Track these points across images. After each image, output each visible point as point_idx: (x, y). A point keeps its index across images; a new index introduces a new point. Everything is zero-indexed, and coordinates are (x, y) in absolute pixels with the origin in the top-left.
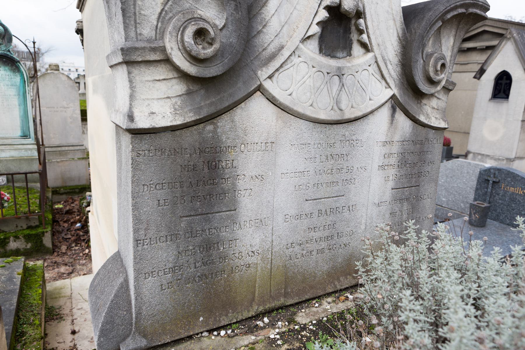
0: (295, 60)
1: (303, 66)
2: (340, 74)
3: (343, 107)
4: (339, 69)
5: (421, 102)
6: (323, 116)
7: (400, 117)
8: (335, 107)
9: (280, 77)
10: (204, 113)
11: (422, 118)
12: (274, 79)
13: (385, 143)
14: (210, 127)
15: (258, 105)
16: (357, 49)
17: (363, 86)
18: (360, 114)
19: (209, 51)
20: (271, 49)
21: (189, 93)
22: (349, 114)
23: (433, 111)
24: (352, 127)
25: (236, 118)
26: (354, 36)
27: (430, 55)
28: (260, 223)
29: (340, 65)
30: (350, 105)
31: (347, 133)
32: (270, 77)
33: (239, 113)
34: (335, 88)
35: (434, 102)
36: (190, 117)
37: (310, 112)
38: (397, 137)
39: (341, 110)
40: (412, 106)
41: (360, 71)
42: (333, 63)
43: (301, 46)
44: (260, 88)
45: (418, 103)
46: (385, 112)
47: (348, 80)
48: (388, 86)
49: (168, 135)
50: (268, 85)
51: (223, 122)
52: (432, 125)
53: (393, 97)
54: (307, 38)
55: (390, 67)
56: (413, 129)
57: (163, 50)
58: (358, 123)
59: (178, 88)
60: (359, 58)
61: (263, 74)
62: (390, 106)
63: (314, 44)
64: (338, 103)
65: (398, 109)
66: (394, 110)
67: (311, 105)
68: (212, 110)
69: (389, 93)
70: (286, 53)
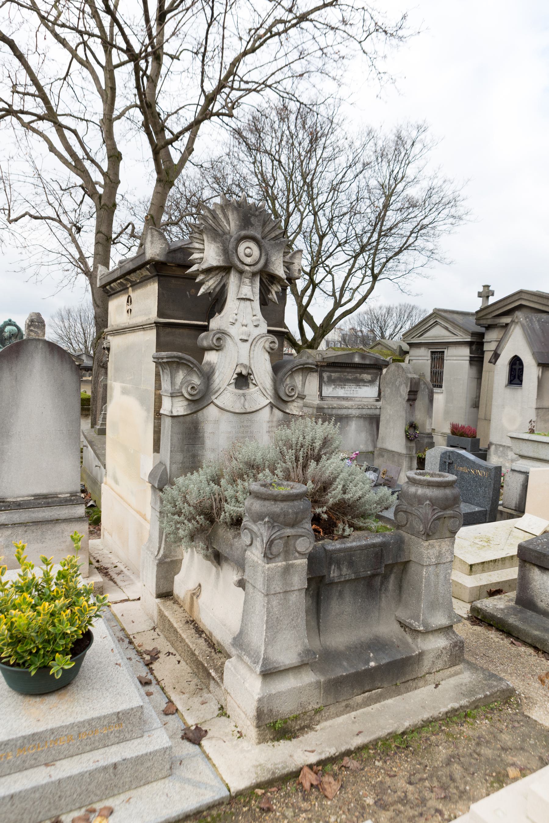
0: (225, 392)
1: (229, 394)
2: (244, 395)
6: (237, 411)
7: (276, 411)
9: (220, 398)
10: (193, 411)
11: (288, 411)
13: (269, 422)
14: (195, 415)
15: (212, 408)
16: (251, 386)
18: (254, 410)
19: (195, 392)
20: (216, 389)
21: (189, 405)
22: (248, 410)
26: (250, 381)
27: (287, 385)
28: (213, 450)
33: (205, 411)
34: (242, 401)
35: (295, 404)
36: (189, 412)
37: (231, 410)
38: (275, 419)
40: (282, 406)
42: (241, 392)
44: (212, 402)
46: (268, 409)
47: (248, 397)
48: (267, 398)
49: (182, 418)
50: (215, 401)
51: (200, 414)
53: (270, 403)
54: (228, 385)
57: (182, 392)
59: (186, 403)
60: (252, 389)
61: (213, 397)
63: (233, 386)
64: (244, 406)
66: (272, 408)
68: (196, 410)
69: (268, 401)
70: (221, 390)
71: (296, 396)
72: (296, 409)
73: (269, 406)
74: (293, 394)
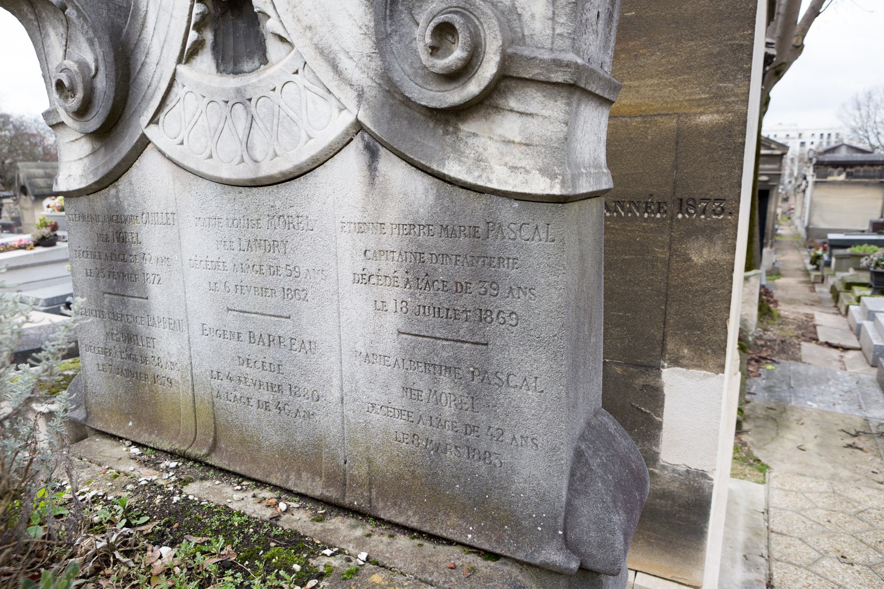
3: (259, 157)
4: (238, 91)
5: (457, 130)
6: (226, 173)
7: (393, 170)
8: (246, 158)
11: (453, 169)
12: (157, 123)
13: (361, 228)
16: (273, 48)
17: (292, 114)
21: (94, 152)
22: (269, 169)
23: (505, 149)
24: (284, 191)
25: (134, 180)
28: (175, 326)
29: (239, 85)
30: (271, 152)
31: (278, 204)
32: (154, 120)
34: (242, 124)
35: (508, 126)
38: (392, 215)
39: (256, 161)
40: (428, 144)
41: (279, 88)
42: (232, 82)
43: (182, 68)
45: (446, 133)
47: (261, 110)
52: (495, 186)
53: (359, 126)
55: (345, 63)
56: (438, 197)
58: (296, 183)
62: (361, 146)
63: (206, 60)
65: (383, 151)
66: (372, 153)
67: (211, 157)
71: (488, 70)
72: (517, 157)
73: (356, 146)
74: (457, 55)
